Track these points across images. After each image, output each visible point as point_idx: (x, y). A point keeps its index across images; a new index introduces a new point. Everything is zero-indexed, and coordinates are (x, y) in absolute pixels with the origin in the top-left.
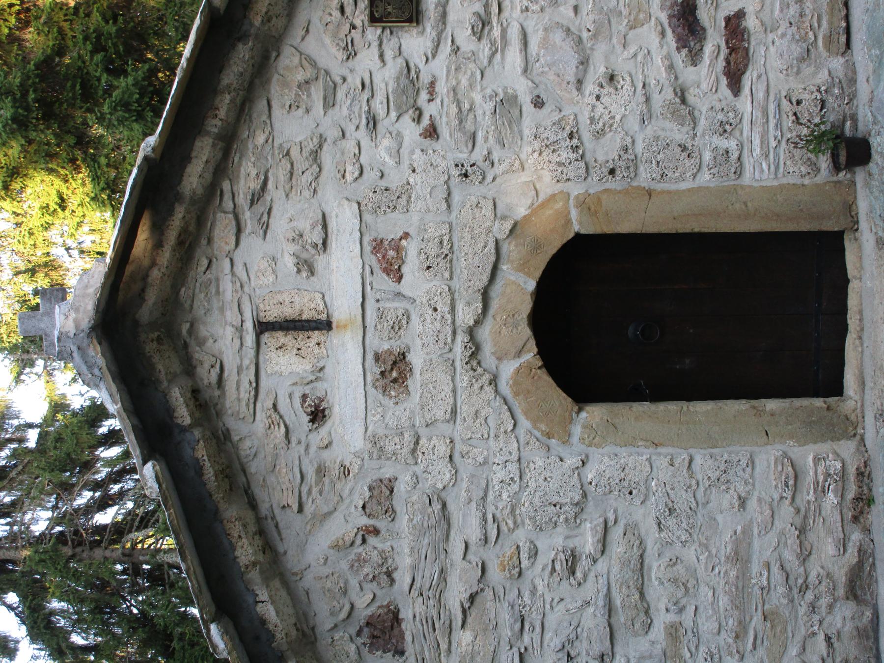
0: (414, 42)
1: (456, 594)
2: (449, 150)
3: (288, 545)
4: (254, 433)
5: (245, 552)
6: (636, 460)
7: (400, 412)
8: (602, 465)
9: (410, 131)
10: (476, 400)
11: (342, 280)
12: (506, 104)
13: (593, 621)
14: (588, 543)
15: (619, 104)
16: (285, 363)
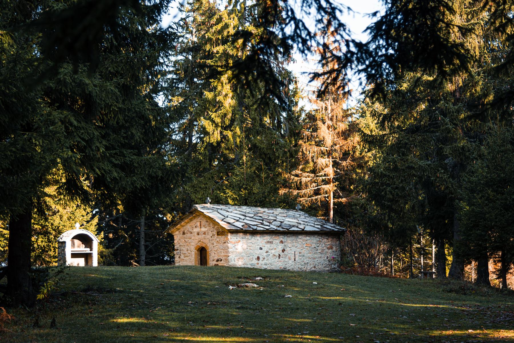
0: (216, 235)
1: (186, 240)
2: (210, 239)
3: (188, 225)
4: (195, 221)
5: (186, 221)
6: (193, 256)
7: (196, 234)
8: (193, 253)
9: (211, 235)
10: (197, 241)
11: (203, 229)
12: (213, 244)
13: (184, 252)
14: (189, 252)
15: (213, 254)
16: (198, 224)
